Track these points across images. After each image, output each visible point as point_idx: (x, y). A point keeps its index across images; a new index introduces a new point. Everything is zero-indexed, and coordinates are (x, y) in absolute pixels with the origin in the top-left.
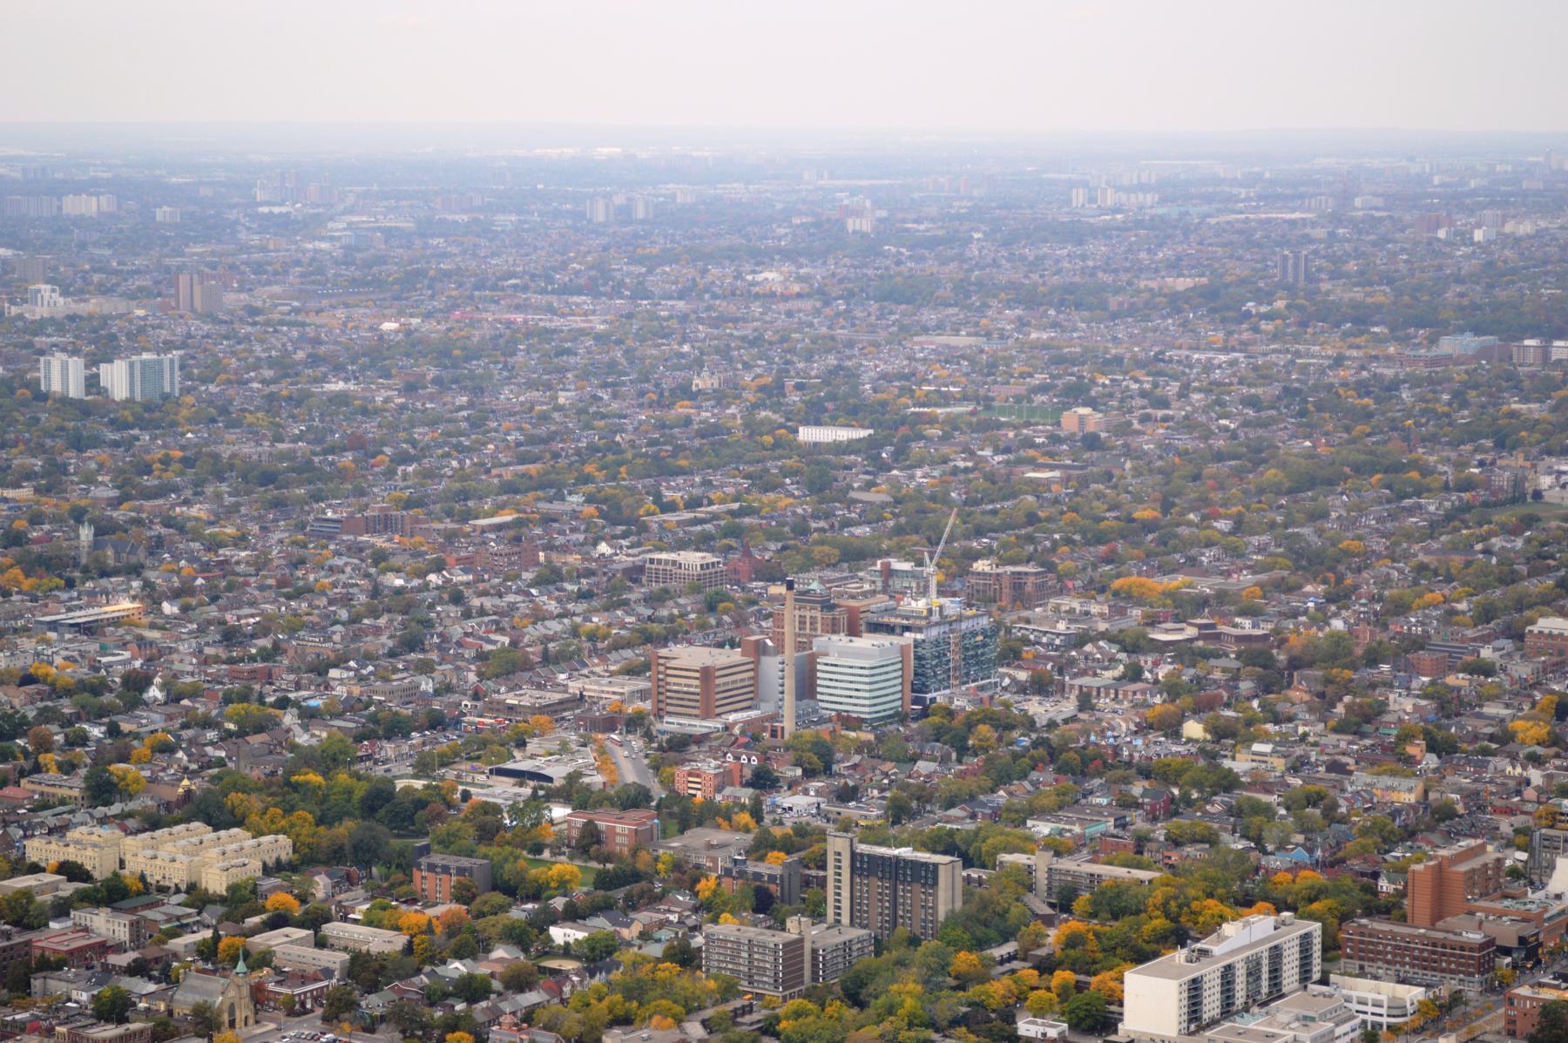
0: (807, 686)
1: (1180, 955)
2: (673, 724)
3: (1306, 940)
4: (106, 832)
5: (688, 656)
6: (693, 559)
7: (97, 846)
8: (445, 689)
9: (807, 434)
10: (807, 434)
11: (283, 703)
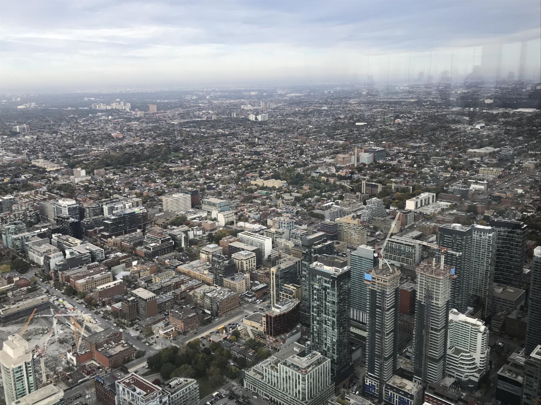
0: (358, 160)
1: (415, 198)
2: (338, 165)
3: (433, 196)
4: (262, 180)
5: (341, 156)
6: (341, 142)
7: (260, 182)
8: (306, 161)
9: (357, 124)
10: (357, 124)
11: (284, 162)
